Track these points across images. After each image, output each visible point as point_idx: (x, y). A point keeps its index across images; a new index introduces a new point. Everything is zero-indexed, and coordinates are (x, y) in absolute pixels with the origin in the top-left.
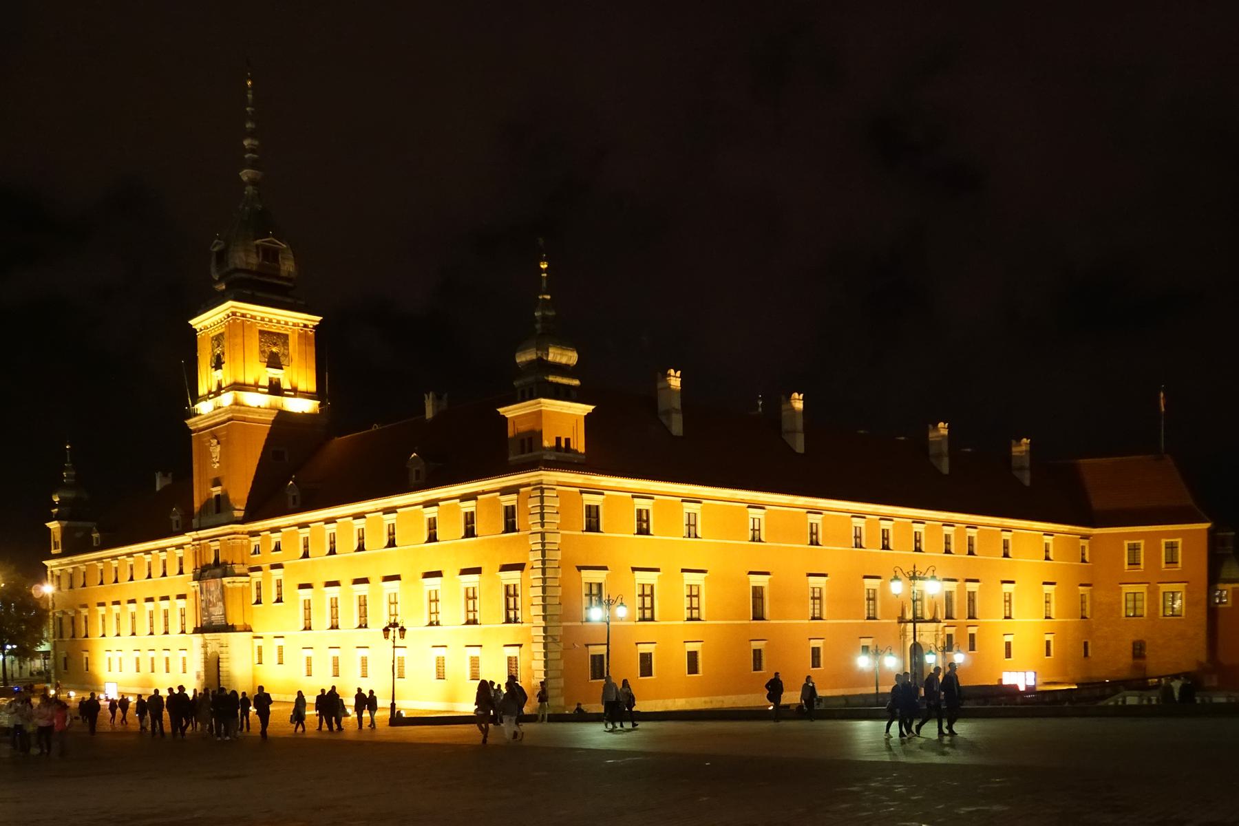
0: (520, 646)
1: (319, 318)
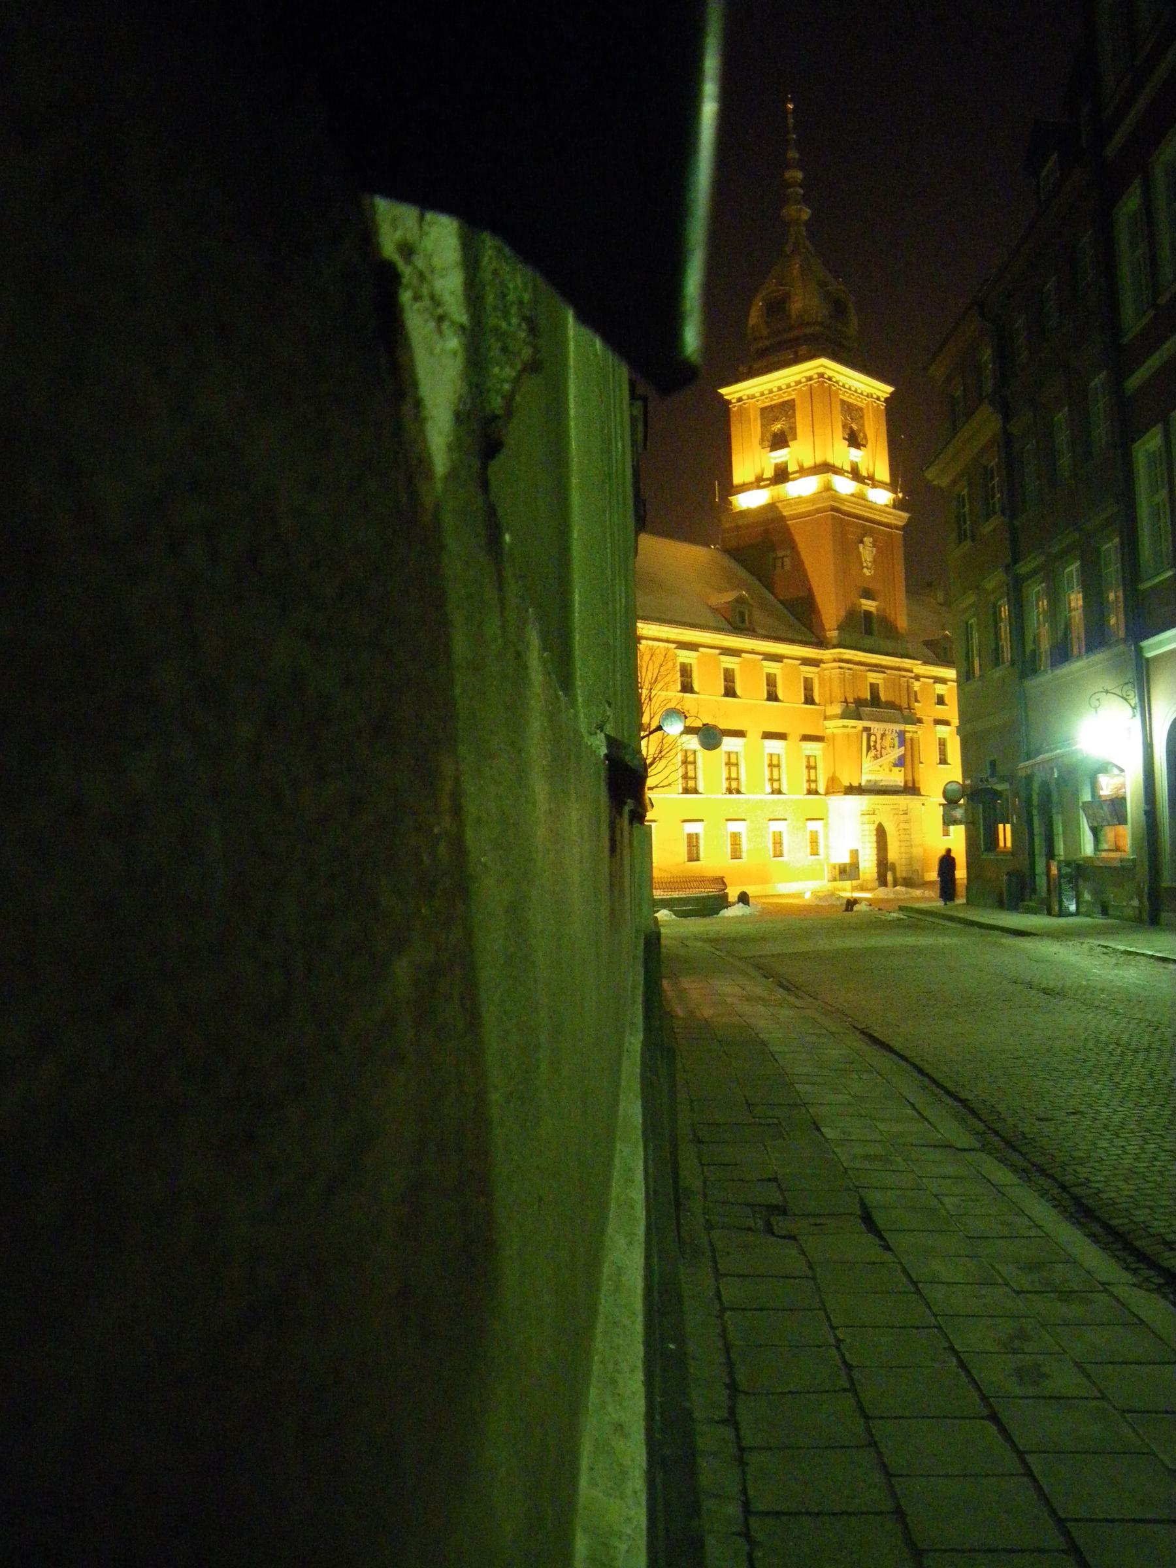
1: (890, 389)
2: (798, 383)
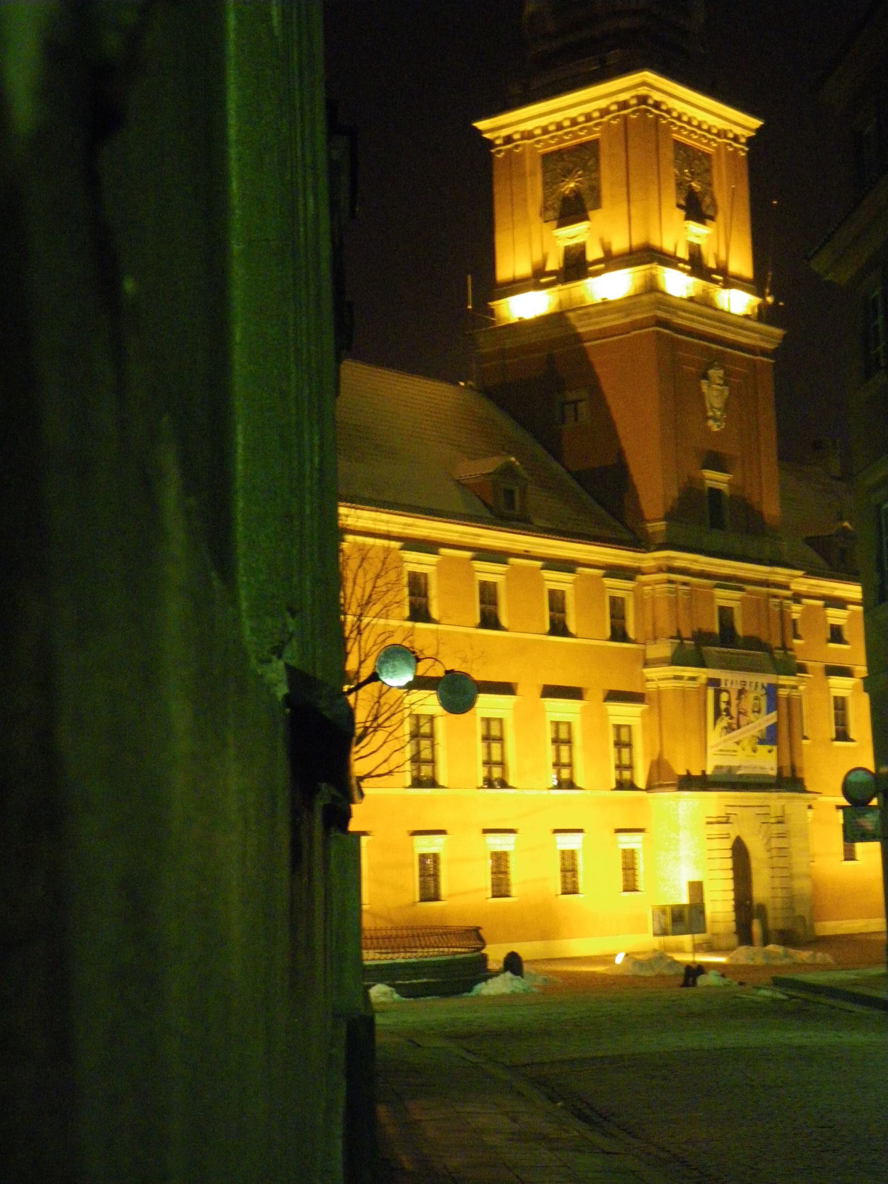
1: (755, 123)
2: (604, 112)
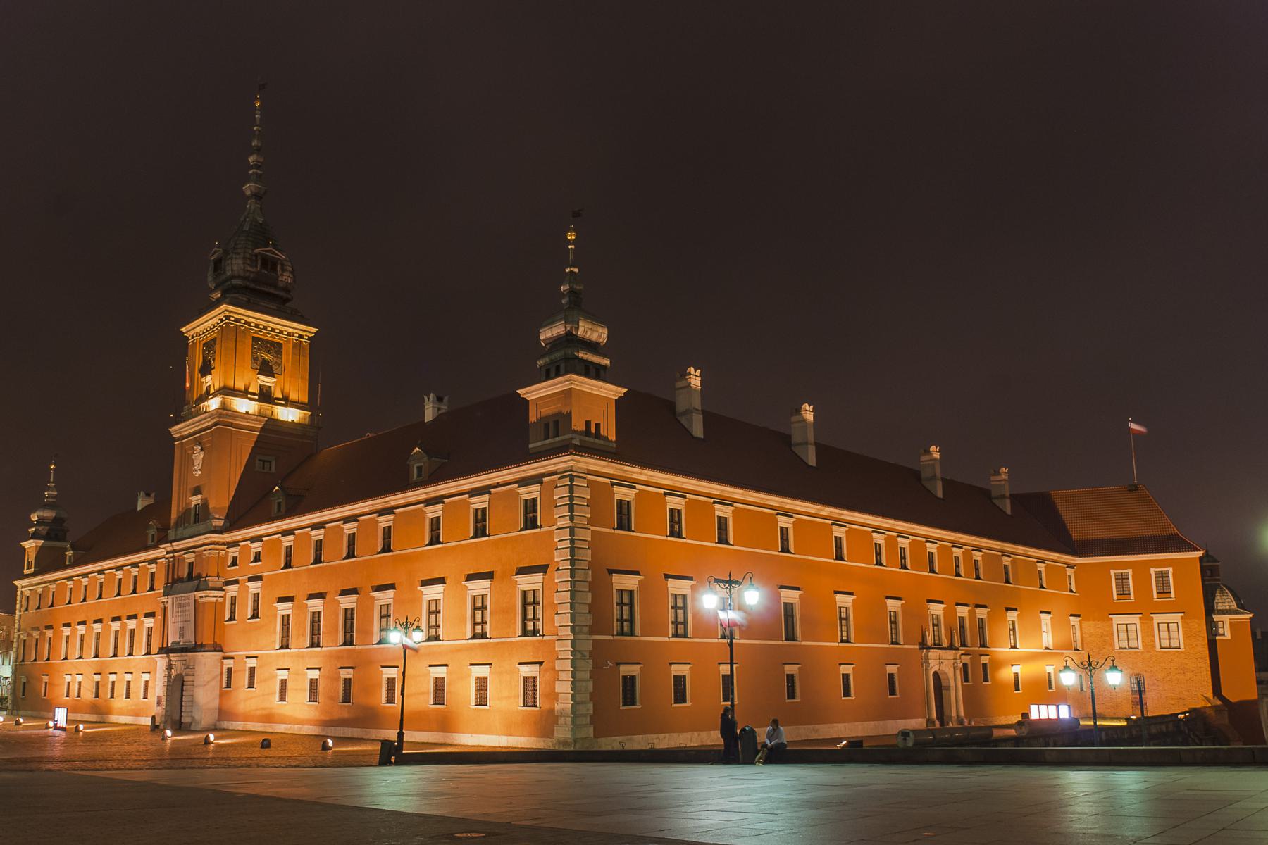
0: (541, 663)
